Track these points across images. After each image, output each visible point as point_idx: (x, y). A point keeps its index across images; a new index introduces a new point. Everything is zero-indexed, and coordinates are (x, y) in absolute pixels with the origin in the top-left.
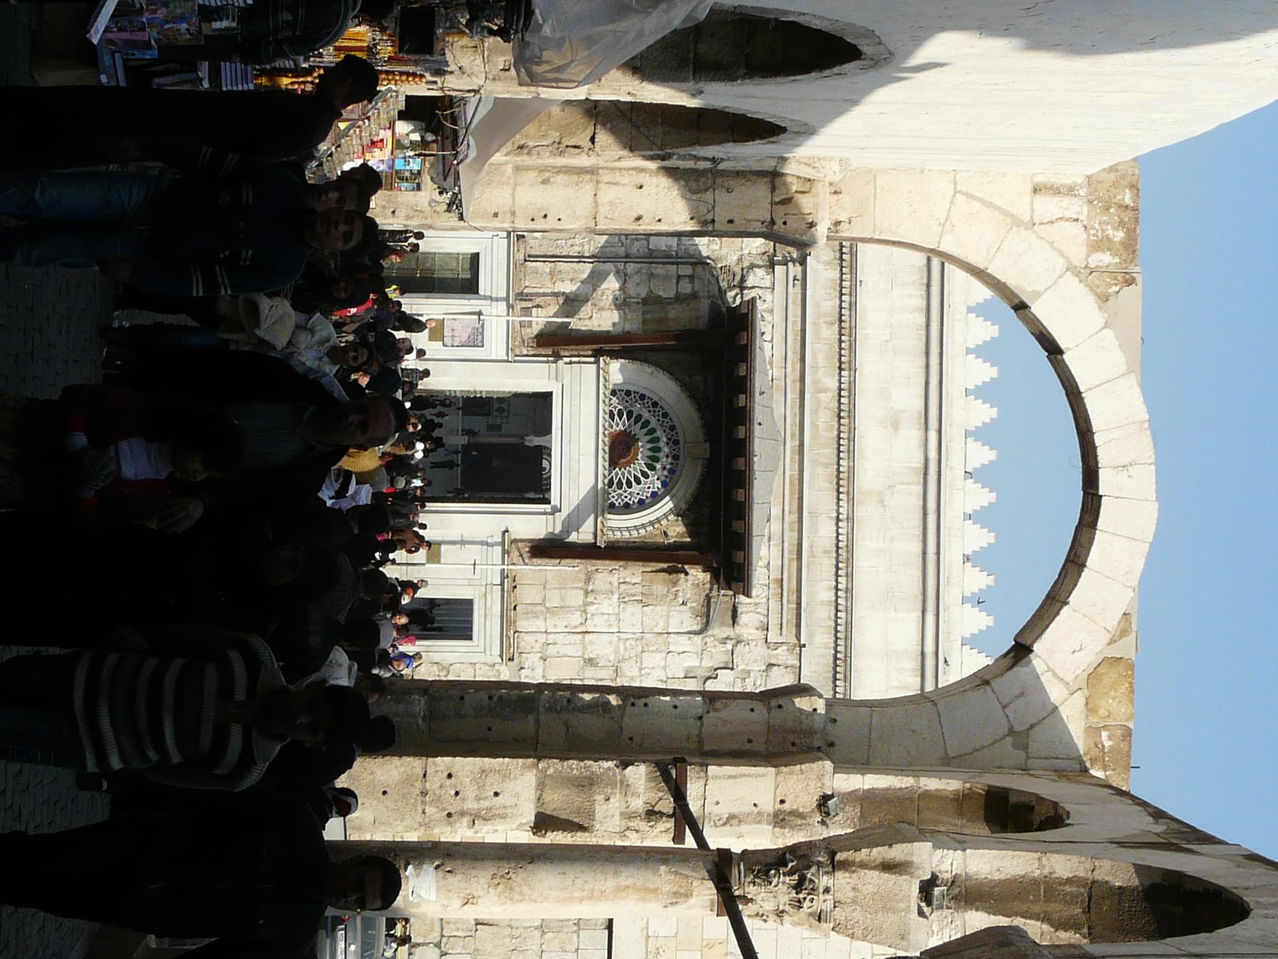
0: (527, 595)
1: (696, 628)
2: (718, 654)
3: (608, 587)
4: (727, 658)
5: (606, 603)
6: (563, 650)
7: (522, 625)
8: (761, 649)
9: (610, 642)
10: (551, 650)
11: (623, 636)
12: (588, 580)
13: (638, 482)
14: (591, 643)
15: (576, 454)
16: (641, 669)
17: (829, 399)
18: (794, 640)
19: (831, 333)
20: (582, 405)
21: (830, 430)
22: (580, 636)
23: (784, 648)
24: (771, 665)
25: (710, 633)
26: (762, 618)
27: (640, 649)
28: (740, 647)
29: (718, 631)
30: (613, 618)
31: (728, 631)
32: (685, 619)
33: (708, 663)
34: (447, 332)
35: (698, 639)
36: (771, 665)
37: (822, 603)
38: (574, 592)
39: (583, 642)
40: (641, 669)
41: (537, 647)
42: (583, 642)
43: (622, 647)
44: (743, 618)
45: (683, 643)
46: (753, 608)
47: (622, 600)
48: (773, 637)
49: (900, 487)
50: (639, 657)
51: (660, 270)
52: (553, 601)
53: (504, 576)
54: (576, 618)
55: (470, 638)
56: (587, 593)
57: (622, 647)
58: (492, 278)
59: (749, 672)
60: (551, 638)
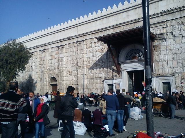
0: (161, 72)
1: (165, 41)
2: (170, 36)
3: (158, 58)
4: (170, 34)
5: (161, 57)
6: (171, 64)
7: (167, 72)
8: (168, 28)
9: (169, 56)
10: (172, 67)
11: (168, 53)
12: (157, 61)
13: (131, 54)
14: (170, 59)
15: (137, 66)
16: (174, 49)
17: (125, 27)
18: (166, 22)
19: (116, 29)
20: (128, 67)
21: (129, 26)
22: (168, 62)
23: (167, 24)
24: (171, 25)
25: (165, 38)
26: (161, 29)
27: (170, 50)
28: (168, 32)
29: (165, 36)
30: (164, 56)
31: (165, 35)
32: (163, 44)
33: (172, 37)
34: (118, 89)
35: (167, 40)
36: (171, 25)
37: (158, 19)
38: (159, 64)
39: (169, 61)
40: (174, 49)
41: (171, 69)
42: (169, 61)
43: (170, 53)
44: (162, 32)
45: (168, 43)
46: (160, 31)
47: (161, 55)
48: (165, 26)
49: (138, 12)
50: (172, 50)
51: (109, 57)
52: (161, 67)
53: (157, 77)
54: (164, 63)
55: (170, 82)
56: (160, 61)
57: (170, 53)
58: (110, 82)
59: (173, 29)
60: (169, 67)
